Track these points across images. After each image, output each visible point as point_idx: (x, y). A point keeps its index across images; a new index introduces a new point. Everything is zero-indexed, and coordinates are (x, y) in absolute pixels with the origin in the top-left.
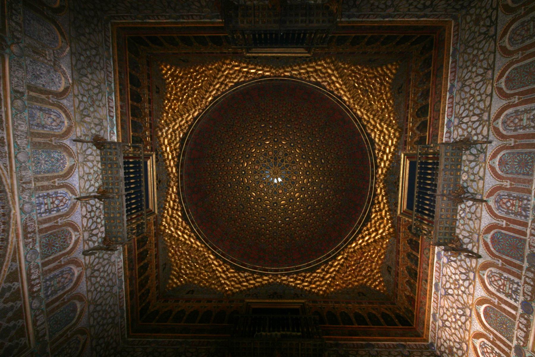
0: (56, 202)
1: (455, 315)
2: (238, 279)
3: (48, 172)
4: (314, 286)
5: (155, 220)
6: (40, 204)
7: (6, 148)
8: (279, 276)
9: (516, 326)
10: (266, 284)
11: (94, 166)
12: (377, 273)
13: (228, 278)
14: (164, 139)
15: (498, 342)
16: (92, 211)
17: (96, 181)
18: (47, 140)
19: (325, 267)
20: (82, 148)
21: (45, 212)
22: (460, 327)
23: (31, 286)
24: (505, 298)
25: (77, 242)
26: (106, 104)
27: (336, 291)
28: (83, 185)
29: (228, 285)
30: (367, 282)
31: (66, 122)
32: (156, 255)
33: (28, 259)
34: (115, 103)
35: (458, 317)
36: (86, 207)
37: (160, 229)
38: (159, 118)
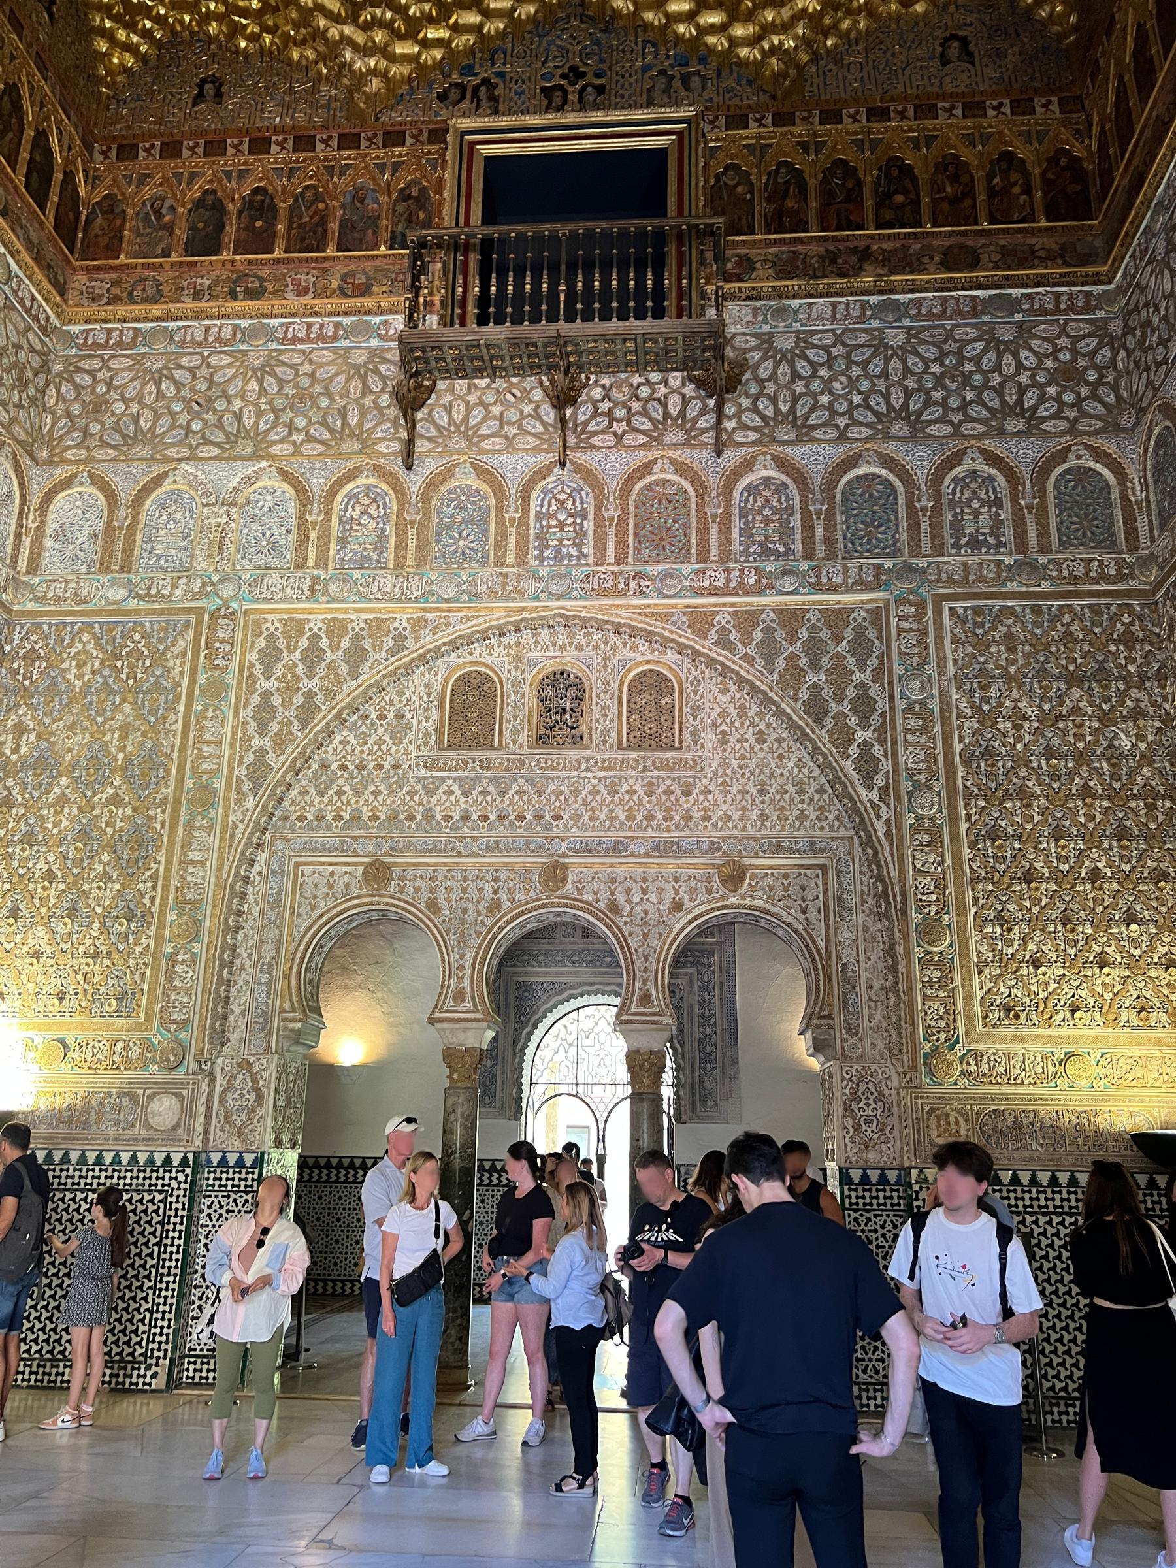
0: (562, 517)
3: (485, 532)
5: (722, 120)
6: (559, 556)
7: (429, 615)
11: (482, 403)
14: (393, 58)
16: (609, 414)
17: (525, 397)
18: (412, 533)
20: (429, 439)
21: (579, 546)
23: (743, 589)
25: (680, 468)
26: (303, 351)
28: (531, 439)
31: (364, 480)
33: (674, 591)
34: (292, 315)
36: (595, 433)
38: (315, 90)
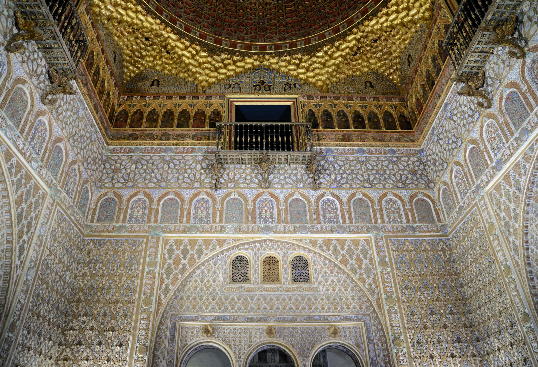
1: (449, 139)
2: (213, 65)
4: (311, 74)
8: (267, 57)
9: (485, 173)
10: (250, 69)
12: (396, 57)
13: (200, 65)
15: (468, 176)
19: (329, 49)
22: (449, 150)
24: (489, 149)
27: (338, 80)
29: (200, 74)
30: (380, 67)
32: (102, 50)
35: (451, 142)
37: (94, 12)
